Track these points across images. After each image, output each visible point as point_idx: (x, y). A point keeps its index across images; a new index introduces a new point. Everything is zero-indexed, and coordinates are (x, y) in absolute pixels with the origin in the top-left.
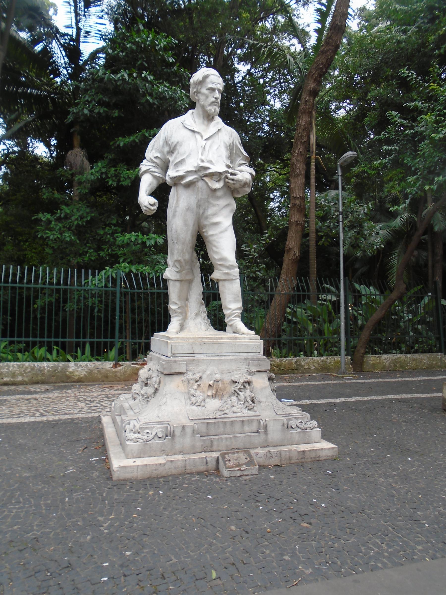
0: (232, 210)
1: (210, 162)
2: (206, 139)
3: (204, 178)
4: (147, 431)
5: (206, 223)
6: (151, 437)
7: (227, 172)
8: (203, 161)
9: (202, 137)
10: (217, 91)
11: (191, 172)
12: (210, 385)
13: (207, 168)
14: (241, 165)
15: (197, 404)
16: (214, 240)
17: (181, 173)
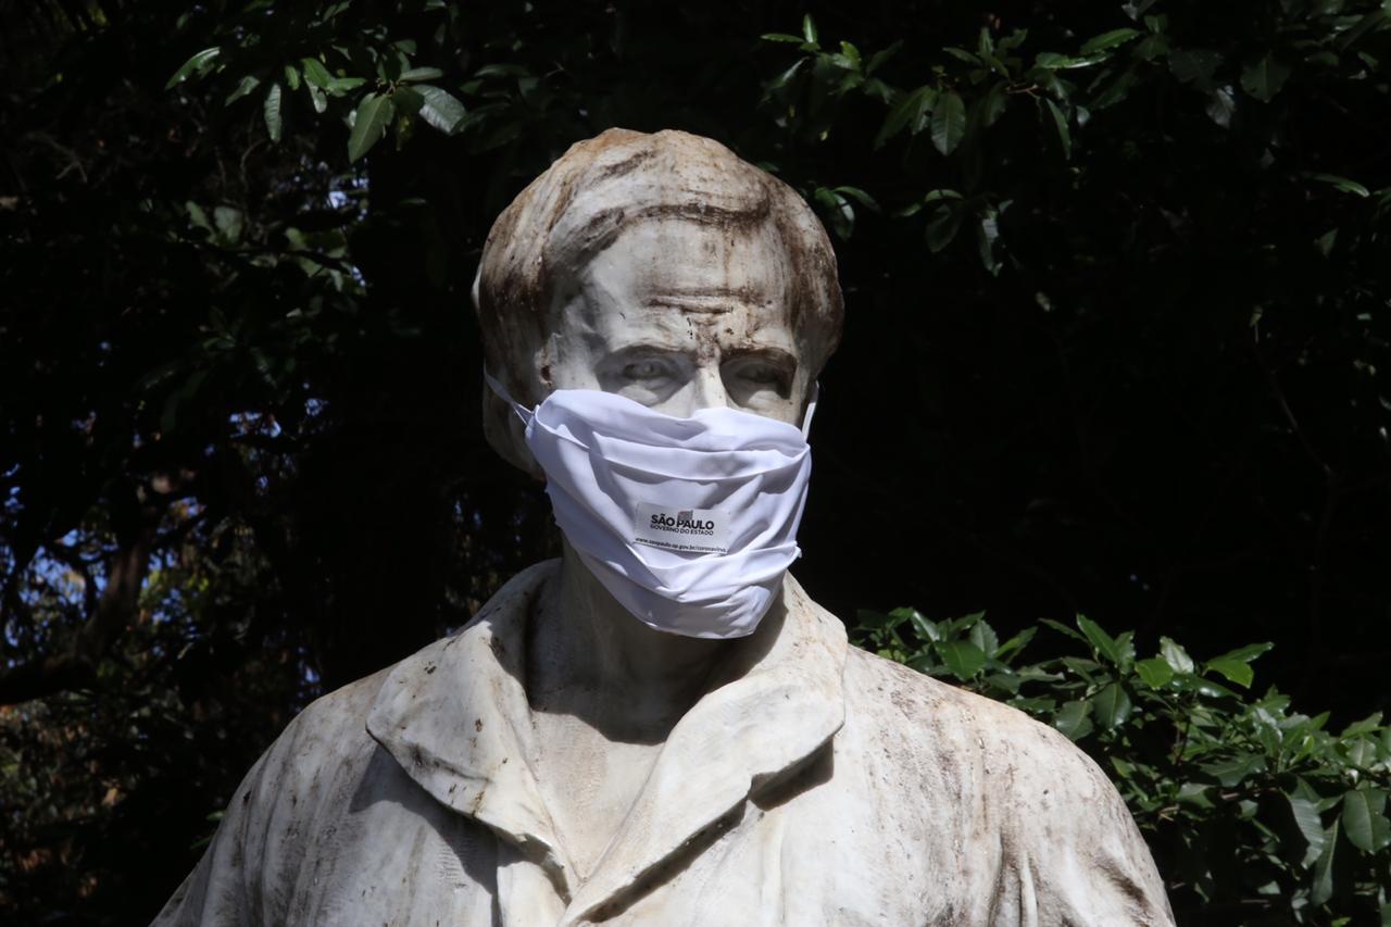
9: (560, 887)
10: (711, 378)
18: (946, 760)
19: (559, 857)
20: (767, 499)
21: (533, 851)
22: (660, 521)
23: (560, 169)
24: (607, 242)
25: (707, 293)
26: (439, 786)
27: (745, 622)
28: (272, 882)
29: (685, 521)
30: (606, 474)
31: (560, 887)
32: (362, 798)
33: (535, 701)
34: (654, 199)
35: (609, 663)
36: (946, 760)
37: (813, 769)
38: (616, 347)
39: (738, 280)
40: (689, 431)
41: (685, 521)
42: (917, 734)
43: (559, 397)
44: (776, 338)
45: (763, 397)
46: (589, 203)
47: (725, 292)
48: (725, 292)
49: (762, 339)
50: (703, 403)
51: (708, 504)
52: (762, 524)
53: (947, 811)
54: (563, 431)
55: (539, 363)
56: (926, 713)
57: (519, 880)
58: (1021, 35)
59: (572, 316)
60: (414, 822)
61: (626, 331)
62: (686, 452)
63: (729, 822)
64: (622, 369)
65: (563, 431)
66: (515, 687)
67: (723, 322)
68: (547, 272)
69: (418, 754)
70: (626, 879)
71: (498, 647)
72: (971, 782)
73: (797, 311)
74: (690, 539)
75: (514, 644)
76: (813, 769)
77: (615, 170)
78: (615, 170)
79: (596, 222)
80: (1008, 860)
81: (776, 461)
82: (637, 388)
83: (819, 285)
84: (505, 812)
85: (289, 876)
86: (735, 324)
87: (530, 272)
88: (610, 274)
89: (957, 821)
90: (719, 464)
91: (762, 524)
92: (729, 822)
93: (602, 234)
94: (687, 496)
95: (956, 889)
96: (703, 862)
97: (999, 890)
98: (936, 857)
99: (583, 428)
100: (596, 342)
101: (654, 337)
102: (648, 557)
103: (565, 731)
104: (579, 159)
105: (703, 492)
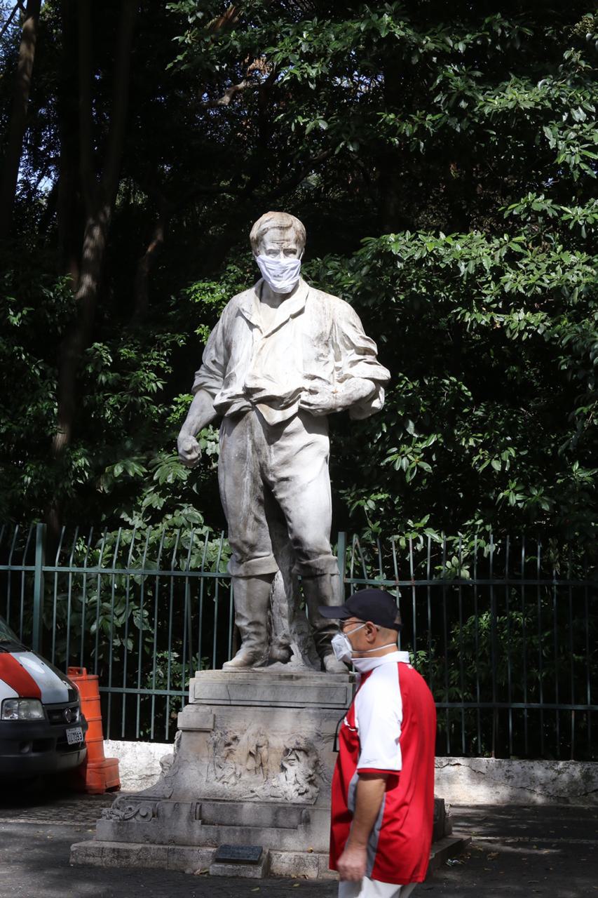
0: (321, 452)
1: (268, 377)
2: (267, 337)
3: (258, 406)
4: (131, 806)
5: (272, 479)
6: (131, 814)
7: (300, 390)
8: (256, 378)
9: (261, 332)
10: (282, 254)
11: (238, 396)
12: (250, 753)
13: (259, 390)
14: (354, 363)
15: (223, 780)
16: (286, 508)
17: (225, 400)
18: (324, 308)
19: (261, 328)
20: (292, 272)
21: (257, 327)
22: (275, 276)
23: (261, 219)
24: (266, 233)
25: (281, 240)
26: (245, 314)
27: (289, 290)
28: (226, 327)
29: (278, 276)
30: (267, 269)
31: (261, 332)
32: (236, 316)
33: (261, 301)
34: (273, 226)
35: (272, 295)
36: (324, 308)
37: (301, 312)
38: (268, 249)
39: (286, 238)
40: (278, 263)
41: (278, 276)
42: (320, 305)
43: (260, 256)
44: (293, 246)
45: (291, 255)
46: (264, 227)
47: (284, 240)
48: (284, 240)
49: (290, 247)
50: (280, 258)
51: (282, 273)
52: (291, 275)
53: (323, 316)
54: (260, 262)
55: (258, 250)
56: (321, 300)
57: (255, 330)
58: (424, 112)
59: (262, 243)
60: (243, 320)
61: (270, 247)
62: (277, 266)
63: (287, 322)
64: (269, 252)
65: (260, 262)
66: (258, 299)
67: (284, 245)
68: (257, 238)
69: (243, 310)
70: (270, 331)
71: (256, 292)
72: (328, 311)
73: (297, 241)
74: (279, 279)
75: (259, 291)
76: (301, 312)
77: (267, 221)
78: (267, 221)
79: (264, 230)
80: (333, 323)
81: (293, 265)
82: (271, 255)
83: (301, 236)
84: (253, 321)
85: (227, 326)
86: (285, 245)
87: (255, 237)
88: (266, 238)
89: (325, 318)
90: (283, 267)
91: (291, 275)
92: (287, 322)
93: (264, 232)
94: (278, 272)
95: (324, 330)
96: (283, 328)
97: (332, 328)
98: (321, 324)
99: (263, 261)
100: (265, 248)
101: (273, 248)
102: (274, 282)
103: (265, 306)
104: (265, 217)
105: (281, 272)
